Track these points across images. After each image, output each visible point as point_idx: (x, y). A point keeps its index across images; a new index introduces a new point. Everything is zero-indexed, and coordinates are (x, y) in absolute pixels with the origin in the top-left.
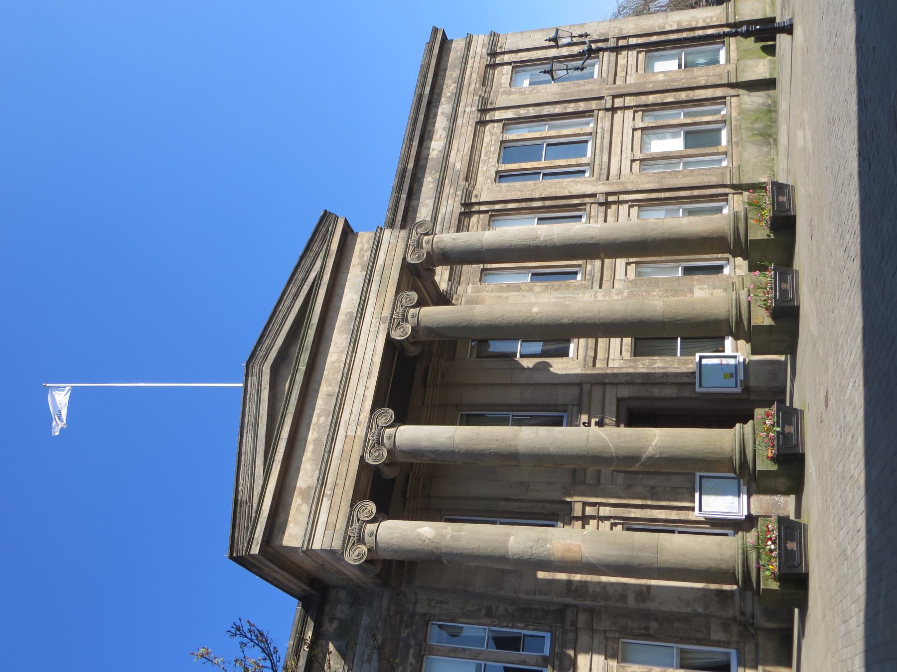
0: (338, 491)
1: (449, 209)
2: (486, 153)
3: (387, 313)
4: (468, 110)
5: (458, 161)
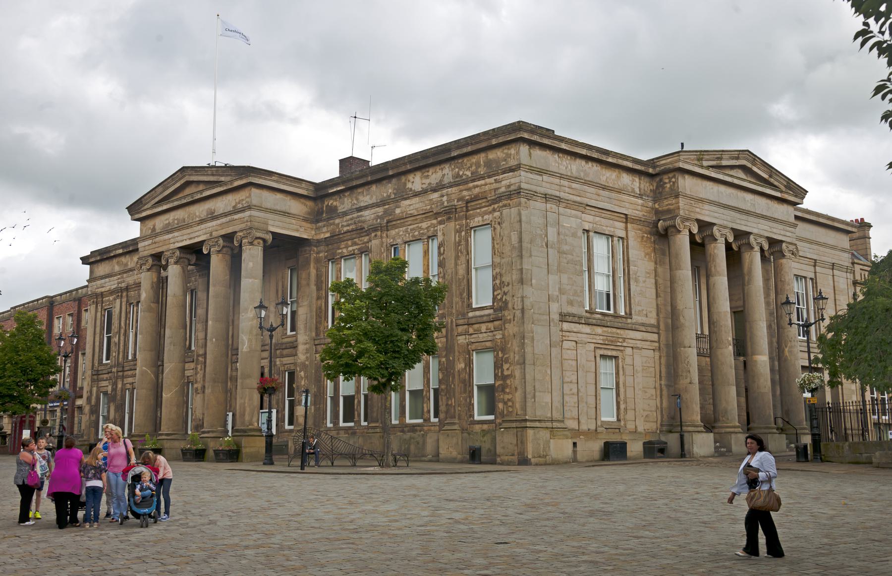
0: (154, 246)
1: (368, 218)
3: (215, 234)
4: (445, 198)
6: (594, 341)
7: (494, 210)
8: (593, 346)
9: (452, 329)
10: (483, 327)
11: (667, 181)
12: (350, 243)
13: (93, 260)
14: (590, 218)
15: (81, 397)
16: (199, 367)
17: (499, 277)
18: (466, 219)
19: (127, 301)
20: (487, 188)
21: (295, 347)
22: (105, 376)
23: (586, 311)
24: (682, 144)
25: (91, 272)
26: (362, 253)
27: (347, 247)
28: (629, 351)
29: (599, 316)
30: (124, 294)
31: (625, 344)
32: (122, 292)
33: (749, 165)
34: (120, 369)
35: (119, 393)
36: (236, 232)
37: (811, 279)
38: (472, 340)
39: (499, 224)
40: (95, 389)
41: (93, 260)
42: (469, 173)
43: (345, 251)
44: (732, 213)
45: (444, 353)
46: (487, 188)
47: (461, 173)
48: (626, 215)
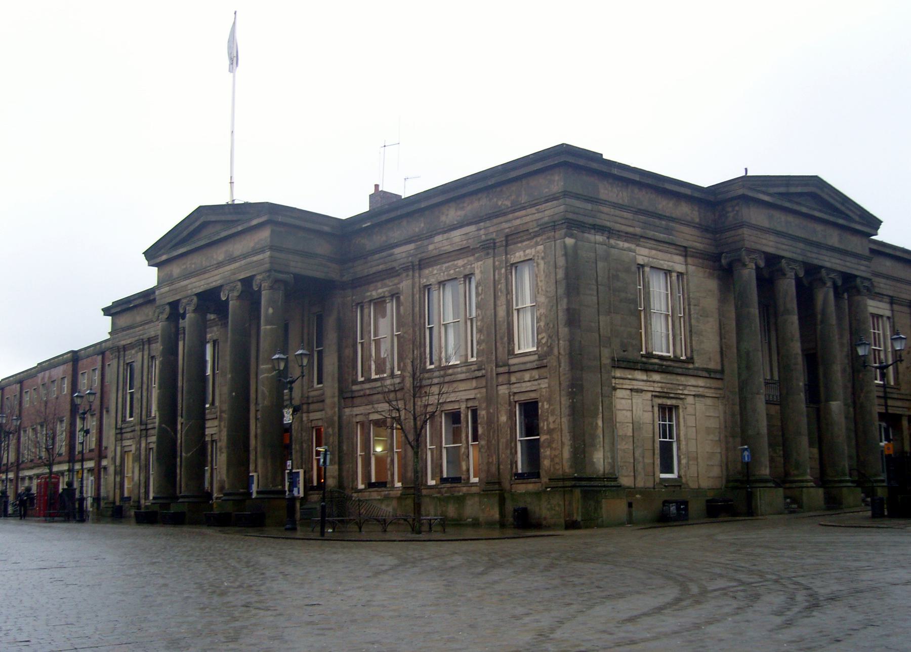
1: (399, 256)
2: (449, 267)
3: (233, 278)
4: (482, 232)
5: (441, 243)
6: (651, 389)
7: (537, 244)
8: (649, 394)
9: (492, 378)
10: (527, 376)
11: (730, 209)
12: (379, 284)
13: (113, 311)
14: (645, 251)
15: (106, 457)
16: (222, 424)
17: (543, 318)
18: (506, 254)
19: (149, 354)
20: (528, 219)
21: (323, 401)
22: (129, 435)
23: (642, 356)
24: (746, 170)
25: (113, 324)
26: (392, 296)
27: (376, 289)
28: (690, 400)
29: (656, 361)
30: (146, 347)
31: (686, 392)
32: (143, 345)
33: (819, 192)
34: (143, 427)
35: (143, 452)
36: (254, 276)
37: (888, 318)
38: (515, 390)
39: (543, 258)
40: (119, 449)
41: (115, 310)
42: (508, 203)
43: (374, 293)
44: (801, 245)
45: (484, 405)
46: (528, 219)
47: (500, 203)
48: (685, 247)
